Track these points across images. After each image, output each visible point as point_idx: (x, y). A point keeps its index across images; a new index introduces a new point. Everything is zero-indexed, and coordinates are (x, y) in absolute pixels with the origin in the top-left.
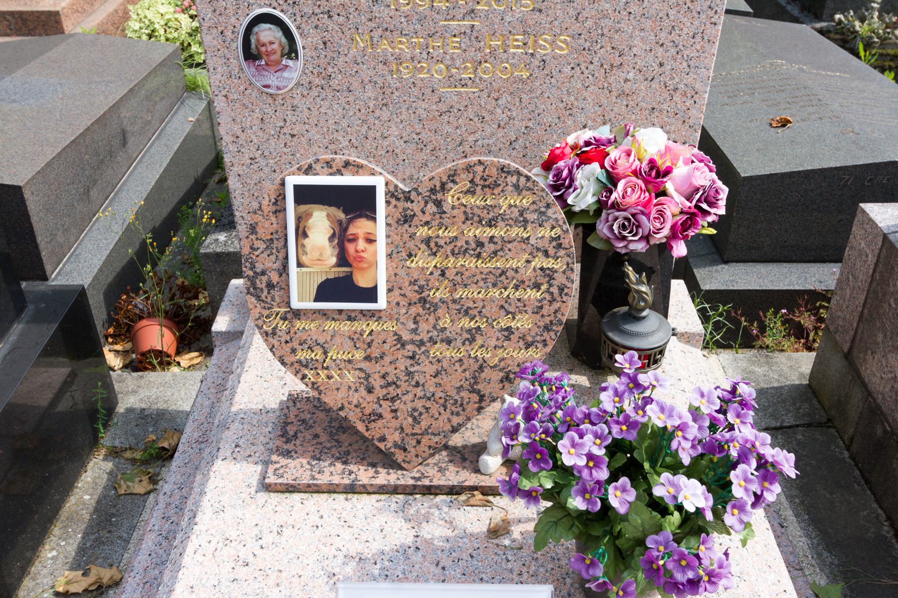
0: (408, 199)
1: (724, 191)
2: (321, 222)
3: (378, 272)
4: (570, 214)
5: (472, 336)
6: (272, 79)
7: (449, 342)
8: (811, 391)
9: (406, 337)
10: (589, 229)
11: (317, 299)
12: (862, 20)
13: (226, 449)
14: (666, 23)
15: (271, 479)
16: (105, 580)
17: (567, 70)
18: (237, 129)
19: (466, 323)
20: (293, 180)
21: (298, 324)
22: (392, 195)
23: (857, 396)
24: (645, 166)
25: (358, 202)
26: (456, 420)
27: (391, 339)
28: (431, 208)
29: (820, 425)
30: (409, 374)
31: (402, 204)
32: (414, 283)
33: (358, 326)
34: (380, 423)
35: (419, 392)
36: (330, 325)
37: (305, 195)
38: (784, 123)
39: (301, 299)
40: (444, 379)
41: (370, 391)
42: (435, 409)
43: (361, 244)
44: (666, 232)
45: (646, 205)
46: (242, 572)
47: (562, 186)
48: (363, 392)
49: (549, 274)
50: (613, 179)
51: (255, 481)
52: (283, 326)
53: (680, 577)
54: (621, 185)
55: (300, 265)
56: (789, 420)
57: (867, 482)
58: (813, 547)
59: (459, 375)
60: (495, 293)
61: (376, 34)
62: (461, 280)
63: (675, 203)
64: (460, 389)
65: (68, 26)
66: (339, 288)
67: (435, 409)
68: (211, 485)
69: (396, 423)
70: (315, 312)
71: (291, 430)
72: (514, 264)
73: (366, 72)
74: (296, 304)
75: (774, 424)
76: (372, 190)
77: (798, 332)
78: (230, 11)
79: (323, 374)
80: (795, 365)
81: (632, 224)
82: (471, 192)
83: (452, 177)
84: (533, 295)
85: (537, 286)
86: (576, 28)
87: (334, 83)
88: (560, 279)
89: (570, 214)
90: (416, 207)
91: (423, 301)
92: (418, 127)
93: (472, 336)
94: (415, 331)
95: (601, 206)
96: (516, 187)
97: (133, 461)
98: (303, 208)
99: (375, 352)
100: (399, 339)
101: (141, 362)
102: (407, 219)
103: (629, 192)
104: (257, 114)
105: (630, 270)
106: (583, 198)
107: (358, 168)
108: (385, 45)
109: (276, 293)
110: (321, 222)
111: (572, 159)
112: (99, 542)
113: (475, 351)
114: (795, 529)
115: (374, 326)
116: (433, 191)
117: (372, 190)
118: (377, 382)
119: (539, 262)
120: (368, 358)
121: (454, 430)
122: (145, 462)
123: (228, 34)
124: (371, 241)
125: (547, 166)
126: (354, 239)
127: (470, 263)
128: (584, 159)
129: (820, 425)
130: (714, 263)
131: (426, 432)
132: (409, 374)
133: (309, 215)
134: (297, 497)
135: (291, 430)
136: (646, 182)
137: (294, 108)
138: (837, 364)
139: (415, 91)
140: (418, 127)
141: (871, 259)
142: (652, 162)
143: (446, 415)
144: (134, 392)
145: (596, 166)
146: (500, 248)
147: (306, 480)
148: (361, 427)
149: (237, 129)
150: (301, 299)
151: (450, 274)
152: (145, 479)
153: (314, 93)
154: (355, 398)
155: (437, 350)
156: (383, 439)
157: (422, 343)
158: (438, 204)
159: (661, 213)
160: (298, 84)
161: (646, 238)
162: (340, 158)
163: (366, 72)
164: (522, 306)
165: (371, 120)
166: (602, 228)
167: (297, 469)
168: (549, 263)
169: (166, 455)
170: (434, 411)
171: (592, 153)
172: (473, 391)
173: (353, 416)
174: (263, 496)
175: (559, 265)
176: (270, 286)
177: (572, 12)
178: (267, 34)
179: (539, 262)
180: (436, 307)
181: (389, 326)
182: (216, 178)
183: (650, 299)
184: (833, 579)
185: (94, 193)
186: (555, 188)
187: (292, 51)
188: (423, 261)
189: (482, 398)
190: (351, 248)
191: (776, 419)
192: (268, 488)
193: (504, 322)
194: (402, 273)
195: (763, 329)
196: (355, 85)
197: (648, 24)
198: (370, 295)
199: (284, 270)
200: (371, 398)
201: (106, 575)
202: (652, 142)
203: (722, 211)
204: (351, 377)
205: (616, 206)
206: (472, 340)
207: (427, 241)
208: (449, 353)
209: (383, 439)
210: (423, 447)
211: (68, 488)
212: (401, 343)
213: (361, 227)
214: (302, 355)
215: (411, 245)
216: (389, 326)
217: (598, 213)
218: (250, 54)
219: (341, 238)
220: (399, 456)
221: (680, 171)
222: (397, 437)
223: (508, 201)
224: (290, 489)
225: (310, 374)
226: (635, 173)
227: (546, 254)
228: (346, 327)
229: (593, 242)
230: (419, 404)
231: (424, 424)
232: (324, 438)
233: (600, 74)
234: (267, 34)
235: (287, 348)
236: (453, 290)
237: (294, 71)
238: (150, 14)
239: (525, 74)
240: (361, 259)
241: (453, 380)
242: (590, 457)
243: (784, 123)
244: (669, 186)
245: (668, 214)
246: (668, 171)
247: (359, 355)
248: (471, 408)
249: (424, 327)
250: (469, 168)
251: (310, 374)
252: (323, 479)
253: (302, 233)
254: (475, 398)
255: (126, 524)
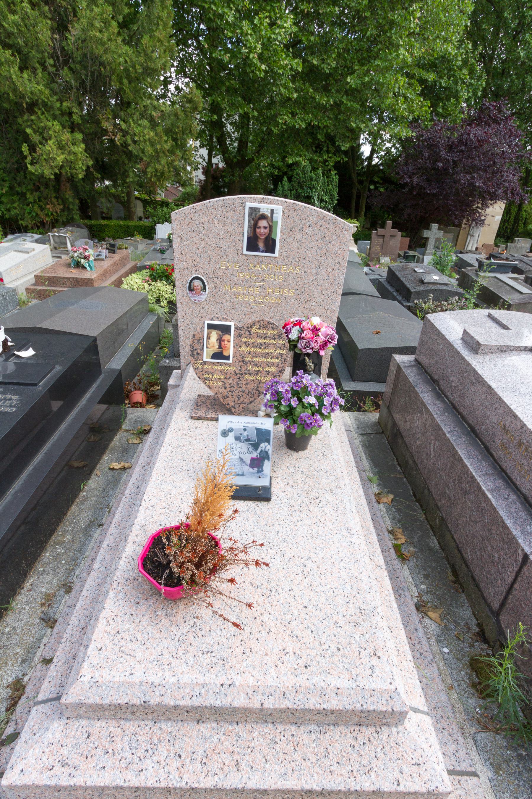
0: (240, 330)
1: (337, 337)
2: (214, 335)
3: (231, 352)
4: (290, 341)
5: (257, 373)
6: (197, 298)
7: (250, 374)
8: (379, 423)
9: (238, 372)
10: (295, 346)
11: (212, 358)
12: (425, 303)
13: (178, 409)
14: (325, 288)
15: (193, 415)
16: (126, 466)
17: (293, 301)
18: (183, 314)
19: (256, 368)
20: (207, 322)
21: (205, 366)
22: (236, 328)
23: (390, 420)
24: (312, 328)
25: (226, 330)
26: (251, 399)
27: (233, 372)
28: (247, 333)
29: (380, 433)
30: (238, 384)
31: (239, 331)
32: (241, 355)
33: (223, 368)
34: (228, 399)
35: (240, 390)
36: (215, 367)
37: (210, 327)
38: (378, 333)
39: (207, 358)
40: (248, 386)
41: (225, 388)
42: (245, 395)
43: (226, 342)
44: (318, 346)
45: (312, 338)
46: (185, 437)
47: (288, 332)
48: (223, 389)
49: (281, 355)
50: (302, 331)
51: (188, 416)
52: (200, 367)
53: (308, 422)
54: (305, 332)
55: (207, 347)
56: (369, 432)
57: (392, 449)
58: (370, 467)
59: (253, 385)
60: (265, 360)
61: (232, 285)
62: (255, 355)
63: (321, 338)
64: (253, 389)
65: (96, 285)
66: (219, 355)
67: (245, 395)
68: (174, 417)
69: (233, 399)
70: (211, 362)
71: (199, 404)
72: (271, 351)
73: (228, 297)
74: (205, 360)
75: (364, 433)
76: (230, 326)
77: (377, 406)
78: (186, 275)
79: (211, 382)
80: (374, 416)
81: (308, 344)
82: (259, 329)
83: (254, 324)
84: (276, 361)
85: (277, 358)
86: (296, 287)
87: (217, 300)
88: (284, 357)
89: (290, 341)
90: (243, 332)
91: (243, 361)
92: (244, 317)
93: (257, 373)
94: (240, 370)
95: (299, 338)
96: (273, 328)
97: (133, 434)
98: (210, 330)
99: (228, 376)
100: (235, 373)
101: (135, 405)
102: (240, 336)
103: (307, 334)
104: (191, 309)
105: (307, 358)
106: (294, 336)
107: (226, 320)
108: (235, 289)
109: (200, 356)
110: (214, 335)
111: (292, 325)
112: (123, 456)
113: (259, 378)
114: (366, 464)
115: (228, 368)
116: (248, 328)
117: (230, 326)
118: (228, 386)
119: (278, 351)
120: (225, 378)
121: (251, 403)
122: (138, 434)
123: (184, 282)
124: (229, 341)
125: (284, 328)
126: (224, 341)
127: (258, 350)
128: (295, 325)
129: (380, 433)
130: (350, 381)
131: (242, 403)
132: (238, 384)
133: (211, 333)
134: (201, 421)
135: (199, 404)
136: (313, 331)
137: (203, 308)
138: (385, 410)
139: (244, 305)
140: (244, 317)
141: (395, 372)
142: (315, 326)
143: (248, 398)
144: (132, 413)
145: (298, 327)
146: (267, 346)
147: (204, 415)
148: (222, 400)
149: (183, 314)
150: (207, 358)
151: (252, 353)
152: (138, 439)
153: (210, 303)
154: (221, 391)
155: (247, 377)
156: (228, 404)
157: (242, 374)
158: (249, 332)
159: (316, 341)
160: (205, 300)
161: (312, 348)
162: (221, 317)
163: (228, 297)
164: (273, 364)
165: (228, 313)
166: (299, 345)
167: (201, 413)
168: (282, 352)
169: (146, 432)
170: (245, 396)
171: (298, 323)
172: (257, 390)
173: (220, 396)
174: (190, 420)
175: (284, 352)
176: (198, 354)
177: (295, 282)
178: (197, 283)
179: (278, 351)
180: (247, 363)
181: (233, 368)
182: (159, 347)
183: (313, 367)
184: (375, 474)
185: (116, 344)
186: (286, 333)
187: (204, 289)
188: (244, 349)
189: (259, 392)
190: (223, 343)
191: (364, 430)
192: (192, 418)
193: (267, 369)
194: (237, 352)
195: (365, 403)
196: (224, 301)
197: (319, 288)
198: (227, 358)
199: (202, 349)
200: (226, 391)
201: (127, 465)
202: (316, 321)
203: (336, 343)
204: (220, 384)
205: (303, 338)
206: (257, 374)
207: (246, 343)
208: (251, 378)
209: (228, 404)
210: (241, 408)
211: (111, 440)
212: (236, 374)
213: (226, 337)
214: (206, 376)
215: (241, 343)
216: (233, 368)
217: (298, 341)
218: (191, 289)
219: (220, 340)
220: (233, 410)
221: (323, 330)
222: (233, 404)
223: (270, 332)
224: (199, 418)
225: (207, 382)
226: (310, 329)
227: (281, 349)
228: (219, 368)
229: (297, 351)
230: (240, 394)
231: (241, 400)
232: (209, 406)
233: (303, 303)
234: (197, 283)
235: (201, 374)
236: (252, 358)
237: (204, 296)
238: (132, 282)
239: (279, 301)
240: (226, 347)
241: (251, 386)
242: (287, 390)
243: (378, 333)
244: (320, 334)
245: (319, 342)
246: (319, 329)
247: (223, 377)
248: (256, 396)
249: (243, 369)
250: (259, 322)
251: (207, 382)
252: (209, 416)
253: (208, 338)
254: (257, 392)
255: (132, 452)
